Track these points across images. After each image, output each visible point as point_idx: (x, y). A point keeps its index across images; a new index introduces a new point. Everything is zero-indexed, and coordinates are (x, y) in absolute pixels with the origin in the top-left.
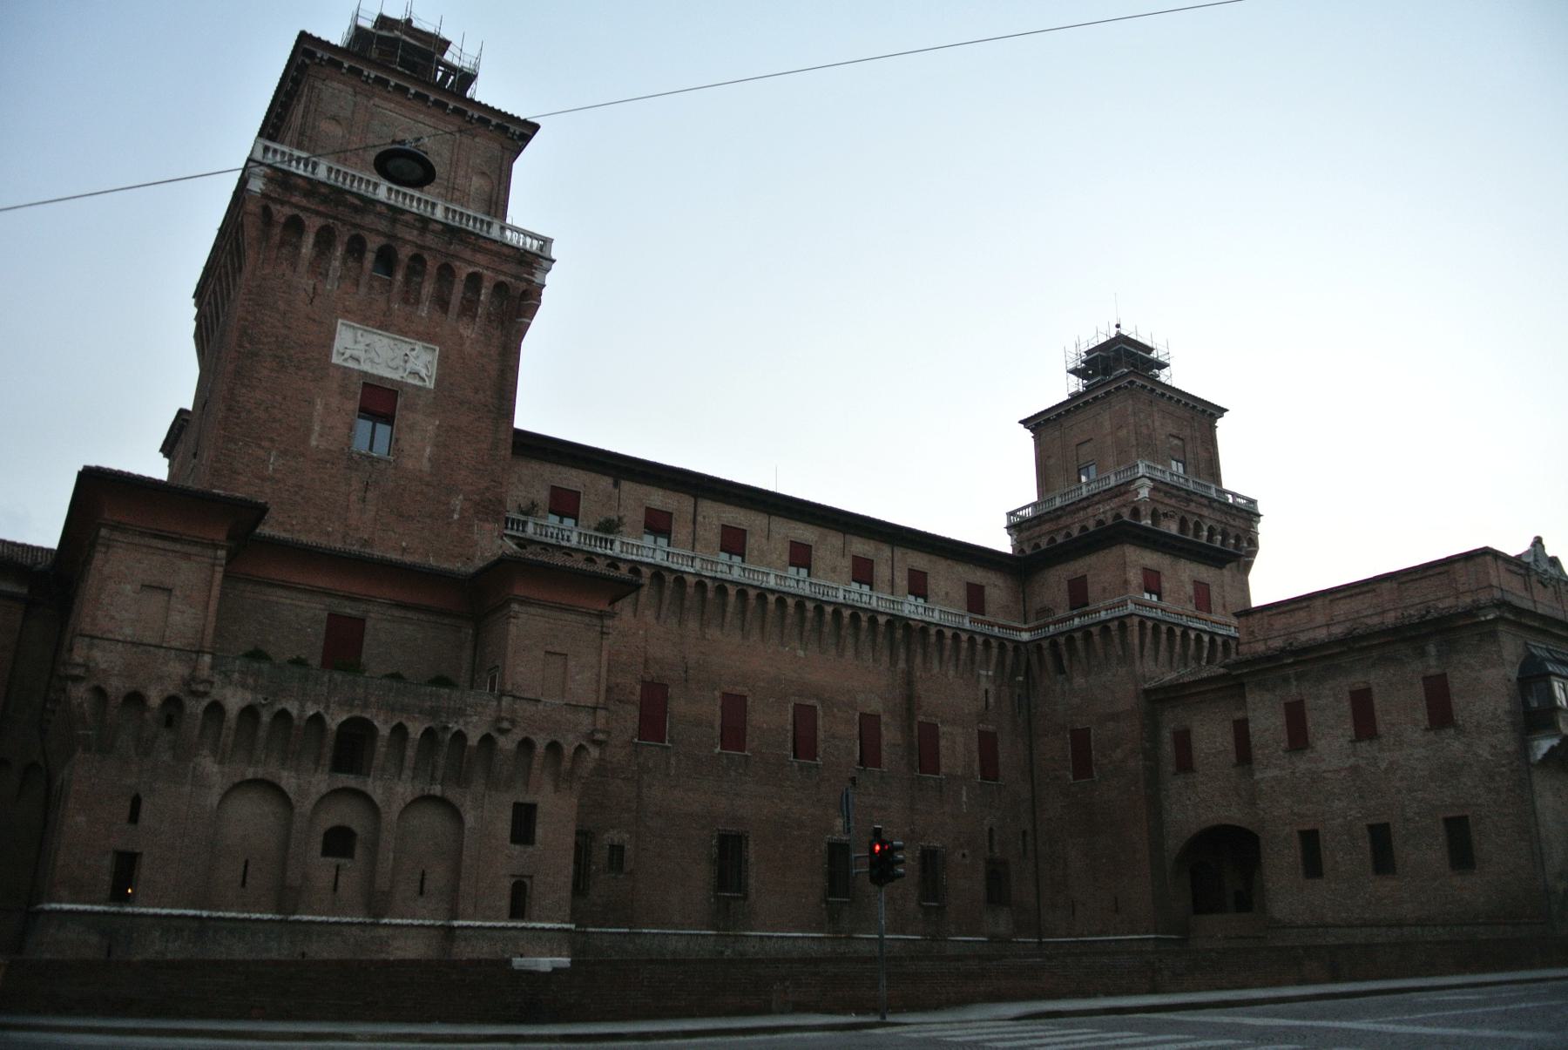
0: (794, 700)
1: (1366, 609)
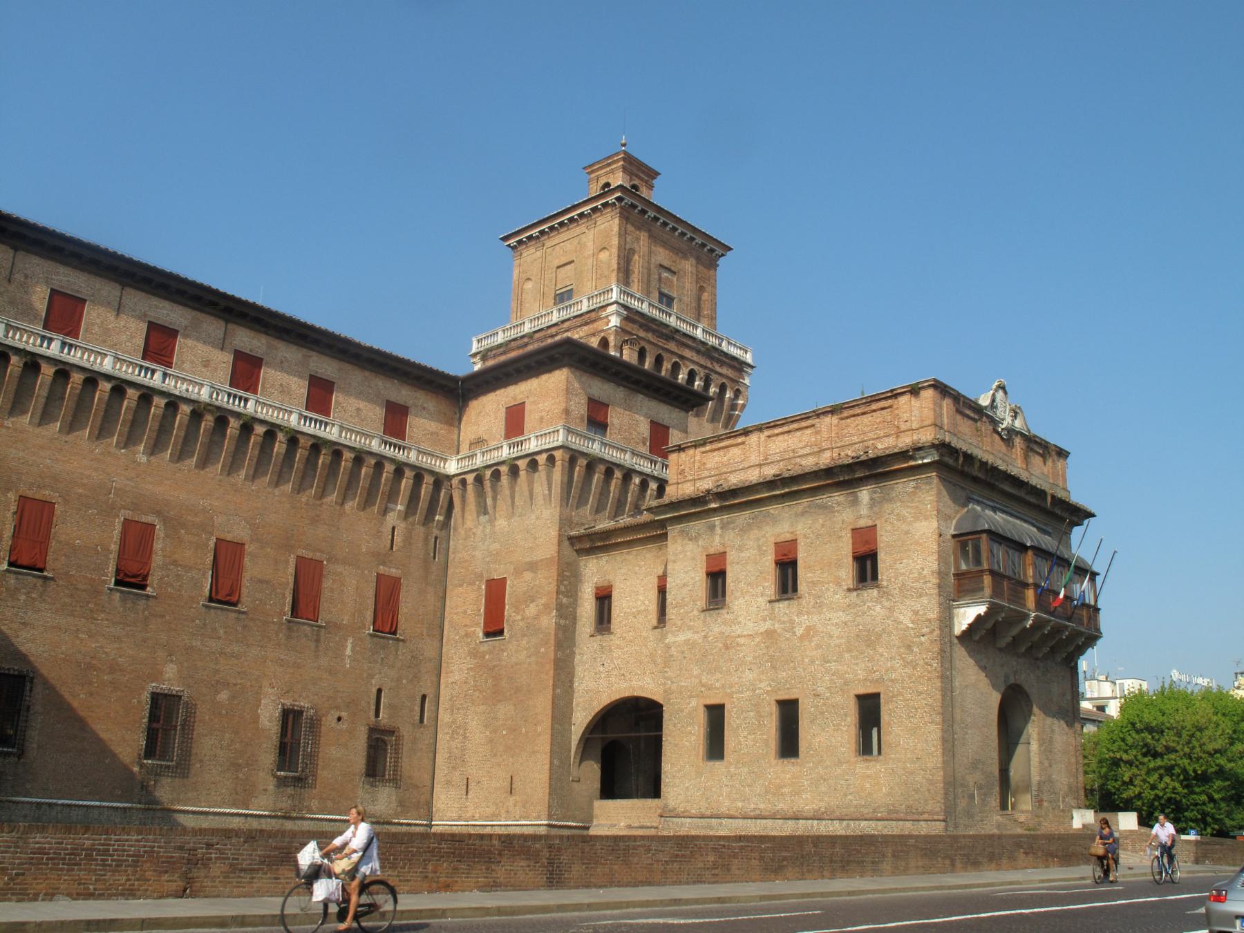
0: (125, 514)
1: (801, 448)
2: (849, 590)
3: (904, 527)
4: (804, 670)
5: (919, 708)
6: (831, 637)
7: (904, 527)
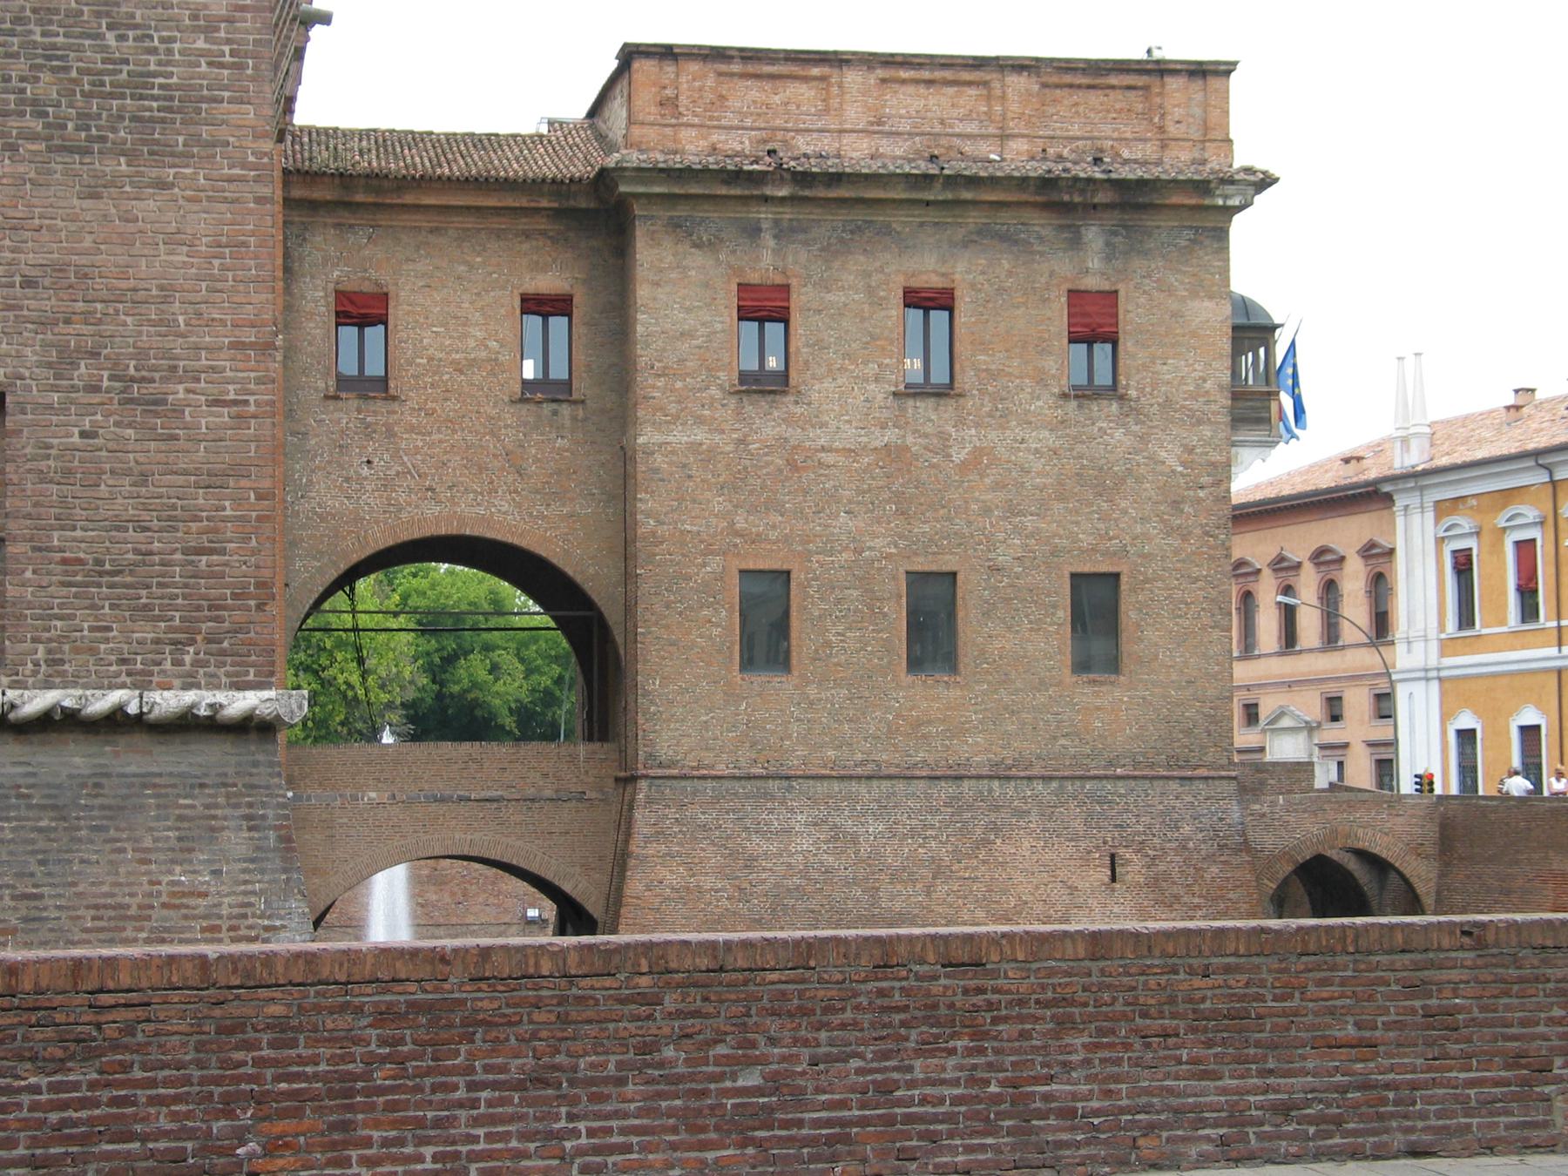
2: (1065, 396)
3: (1173, 305)
4: (970, 523)
5: (1192, 603)
6: (1025, 471)
7: (1173, 305)
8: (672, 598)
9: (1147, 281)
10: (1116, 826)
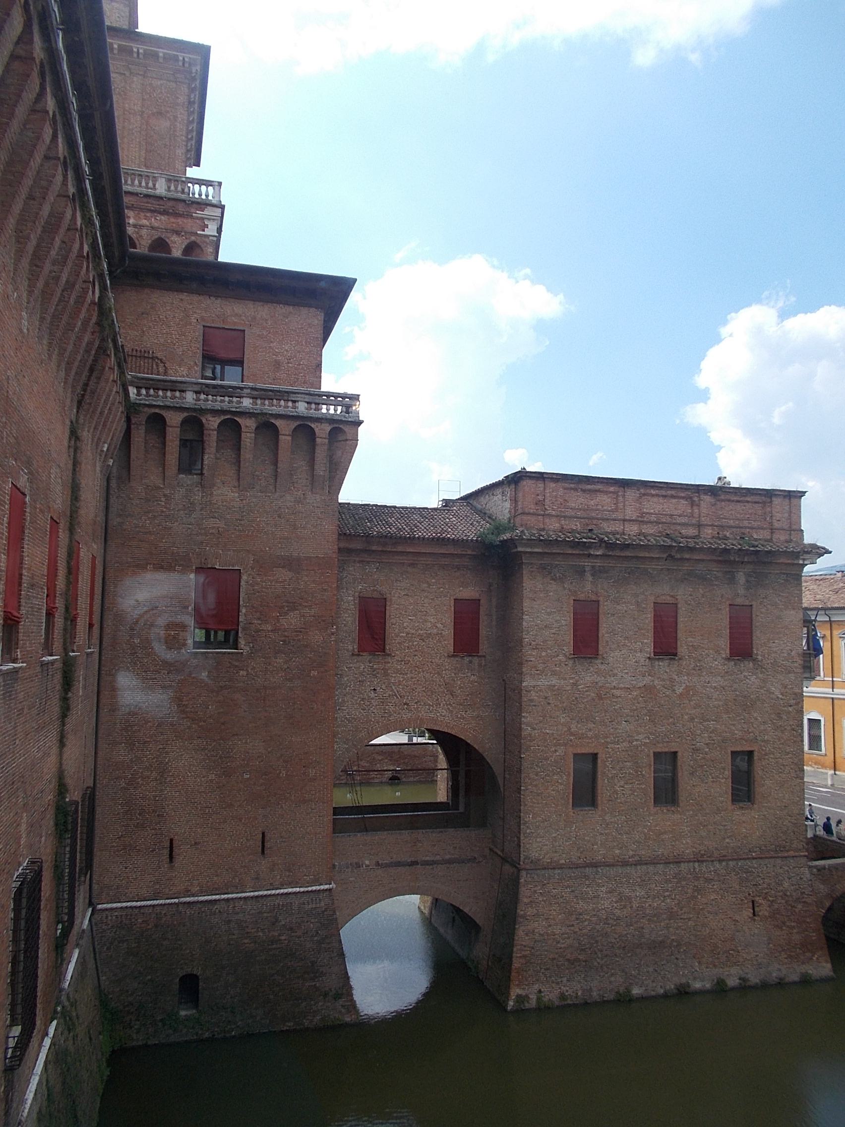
4: (684, 725)
5: (787, 765)
6: (709, 698)
8: (539, 770)
9: (765, 600)
10: (754, 885)
